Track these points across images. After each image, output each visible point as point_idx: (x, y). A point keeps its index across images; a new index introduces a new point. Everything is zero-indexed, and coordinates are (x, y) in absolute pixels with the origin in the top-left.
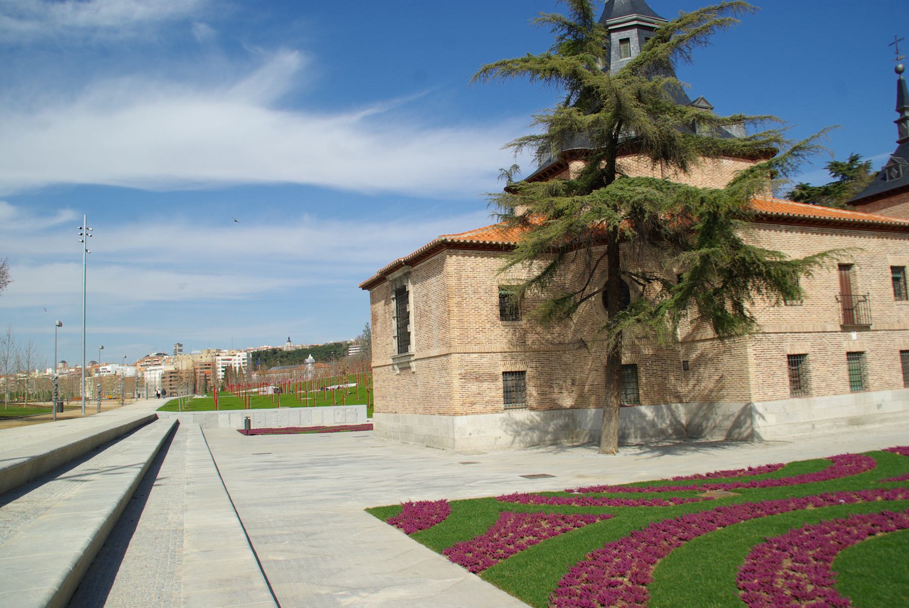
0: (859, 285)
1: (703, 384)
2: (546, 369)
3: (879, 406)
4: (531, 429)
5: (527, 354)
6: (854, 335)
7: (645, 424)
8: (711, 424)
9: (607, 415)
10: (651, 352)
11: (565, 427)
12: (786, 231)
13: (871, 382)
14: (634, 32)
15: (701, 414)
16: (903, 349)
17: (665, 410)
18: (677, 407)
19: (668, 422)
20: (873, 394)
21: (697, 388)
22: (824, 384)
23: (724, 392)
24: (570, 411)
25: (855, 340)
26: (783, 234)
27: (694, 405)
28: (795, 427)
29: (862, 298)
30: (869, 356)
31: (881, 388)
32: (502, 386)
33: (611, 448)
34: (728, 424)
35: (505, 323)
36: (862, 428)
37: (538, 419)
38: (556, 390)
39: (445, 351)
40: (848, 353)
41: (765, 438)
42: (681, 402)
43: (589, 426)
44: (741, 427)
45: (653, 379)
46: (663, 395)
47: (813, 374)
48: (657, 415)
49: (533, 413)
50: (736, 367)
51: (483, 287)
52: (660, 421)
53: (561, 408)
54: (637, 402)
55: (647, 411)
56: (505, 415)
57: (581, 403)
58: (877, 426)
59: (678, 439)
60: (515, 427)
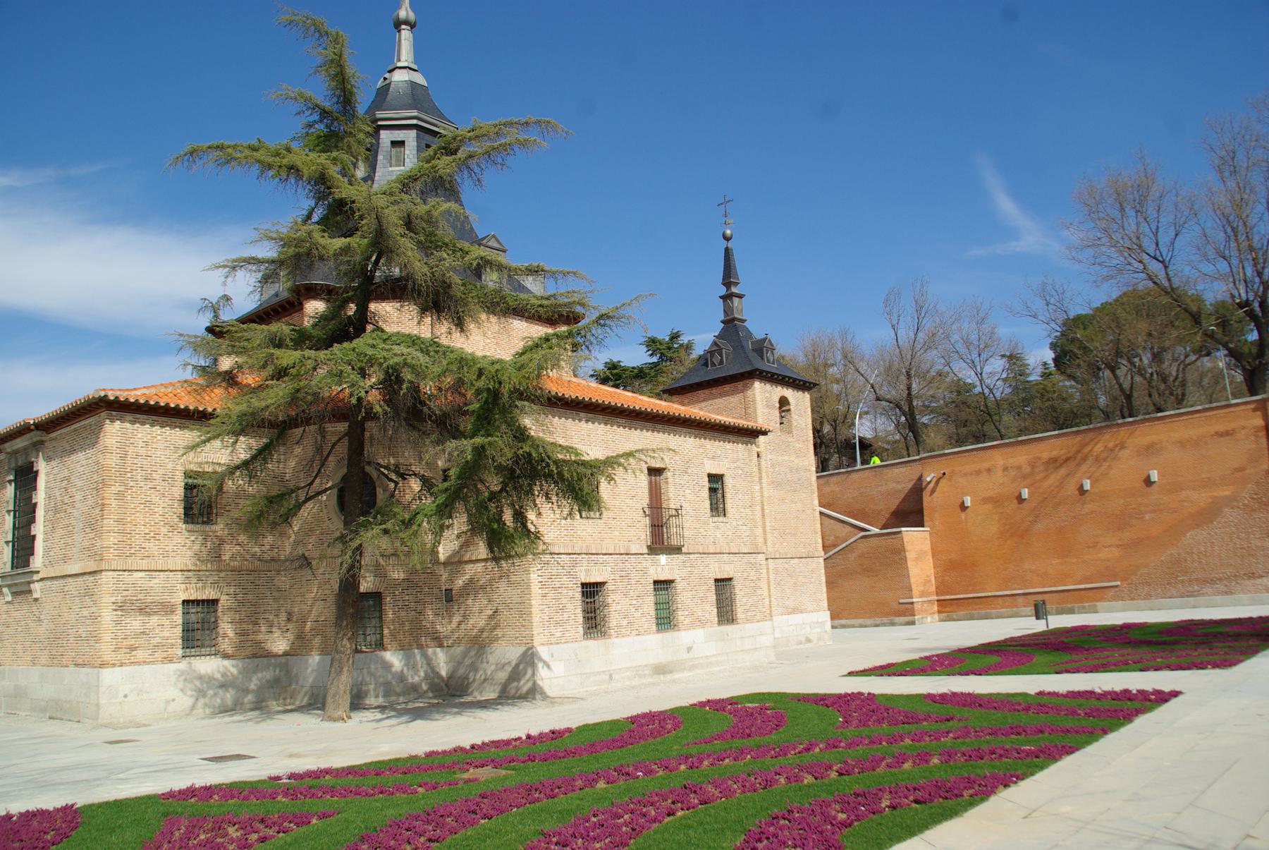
0: (671, 495)
1: (471, 622)
2: (250, 597)
3: (689, 649)
4: (223, 686)
5: (222, 574)
6: (663, 559)
7: (390, 677)
8: (480, 675)
9: (336, 665)
10: (402, 576)
11: (275, 682)
12: (587, 421)
13: (681, 618)
14: (413, 133)
15: (468, 662)
16: (719, 577)
17: (418, 657)
18: (435, 653)
19: (422, 674)
21: (463, 627)
22: (625, 622)
23: (499, 632)
24: (283, 660)
25: (664, 566)
27: (459, 650)
28: (589, 677)
29: (674, 512)
30: (680, 586)
31: (692, 626)
32: (180, 621)
33: (340, 713)
34: (503, 676)
35: (191, 526)
36: (669, 677)
37: (234, 671)
38: (263, 629)
39: (92, 566)
40: (656, 582)
41: (550, 693)
42: (441, 646)
43: (311, 680)
44: (519, 680)
45: (403, 614)
46: (416, 637)
47: (612, 608)
48: (407, 665)
49: (227, 663)
50: (516, 599)
51: (161, 472)
52: (411, 672)
53: (269, 655)
54: (380, 645)
55: (394, 659)
56: (183, 665)
57: (300, 646)
58: (686, 674)
59: (435, 697)
60: (198, 683)
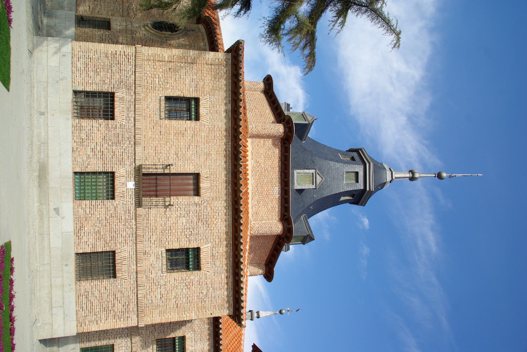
6: (131, 185)
12: (226, 111)
16: (117, 257)
20: (71, 204)
22: (83, 136)
25: (126, 185)
26: (223, 108)
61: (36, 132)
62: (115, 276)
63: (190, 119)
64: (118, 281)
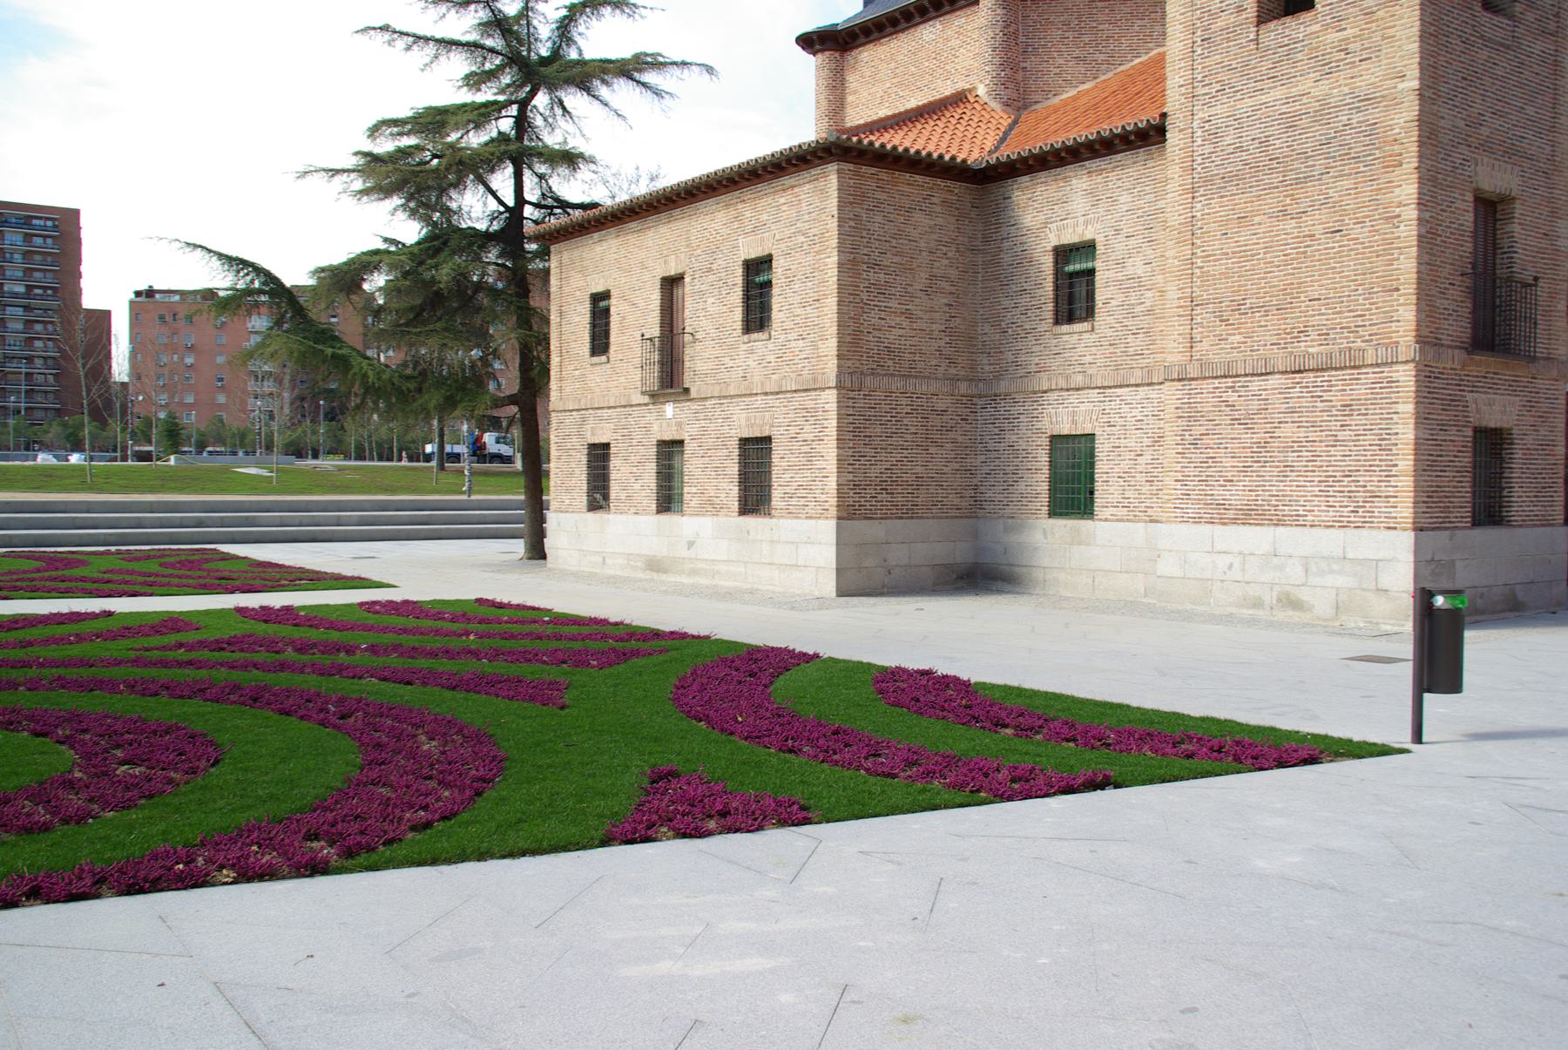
3: (691, 544)
25: (670, 418)
30: (689, 448)
61: (619, 573)
62: (768, 439)
63: (1091, 272)
64: (775, 433)
